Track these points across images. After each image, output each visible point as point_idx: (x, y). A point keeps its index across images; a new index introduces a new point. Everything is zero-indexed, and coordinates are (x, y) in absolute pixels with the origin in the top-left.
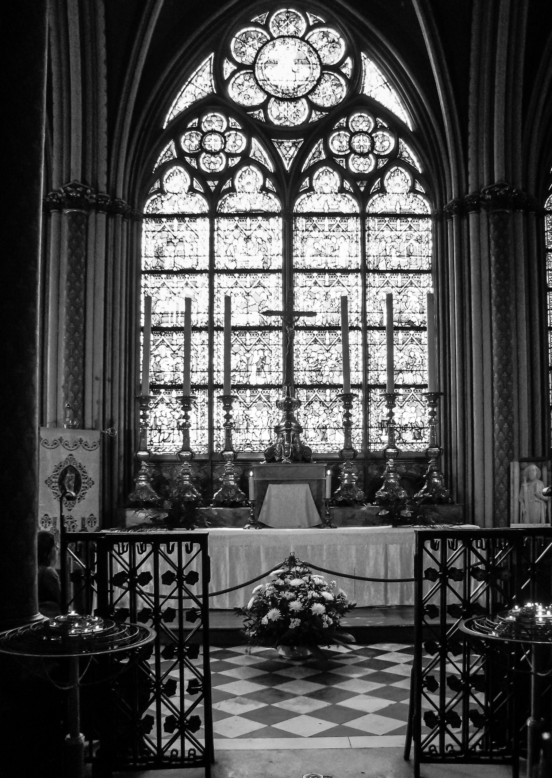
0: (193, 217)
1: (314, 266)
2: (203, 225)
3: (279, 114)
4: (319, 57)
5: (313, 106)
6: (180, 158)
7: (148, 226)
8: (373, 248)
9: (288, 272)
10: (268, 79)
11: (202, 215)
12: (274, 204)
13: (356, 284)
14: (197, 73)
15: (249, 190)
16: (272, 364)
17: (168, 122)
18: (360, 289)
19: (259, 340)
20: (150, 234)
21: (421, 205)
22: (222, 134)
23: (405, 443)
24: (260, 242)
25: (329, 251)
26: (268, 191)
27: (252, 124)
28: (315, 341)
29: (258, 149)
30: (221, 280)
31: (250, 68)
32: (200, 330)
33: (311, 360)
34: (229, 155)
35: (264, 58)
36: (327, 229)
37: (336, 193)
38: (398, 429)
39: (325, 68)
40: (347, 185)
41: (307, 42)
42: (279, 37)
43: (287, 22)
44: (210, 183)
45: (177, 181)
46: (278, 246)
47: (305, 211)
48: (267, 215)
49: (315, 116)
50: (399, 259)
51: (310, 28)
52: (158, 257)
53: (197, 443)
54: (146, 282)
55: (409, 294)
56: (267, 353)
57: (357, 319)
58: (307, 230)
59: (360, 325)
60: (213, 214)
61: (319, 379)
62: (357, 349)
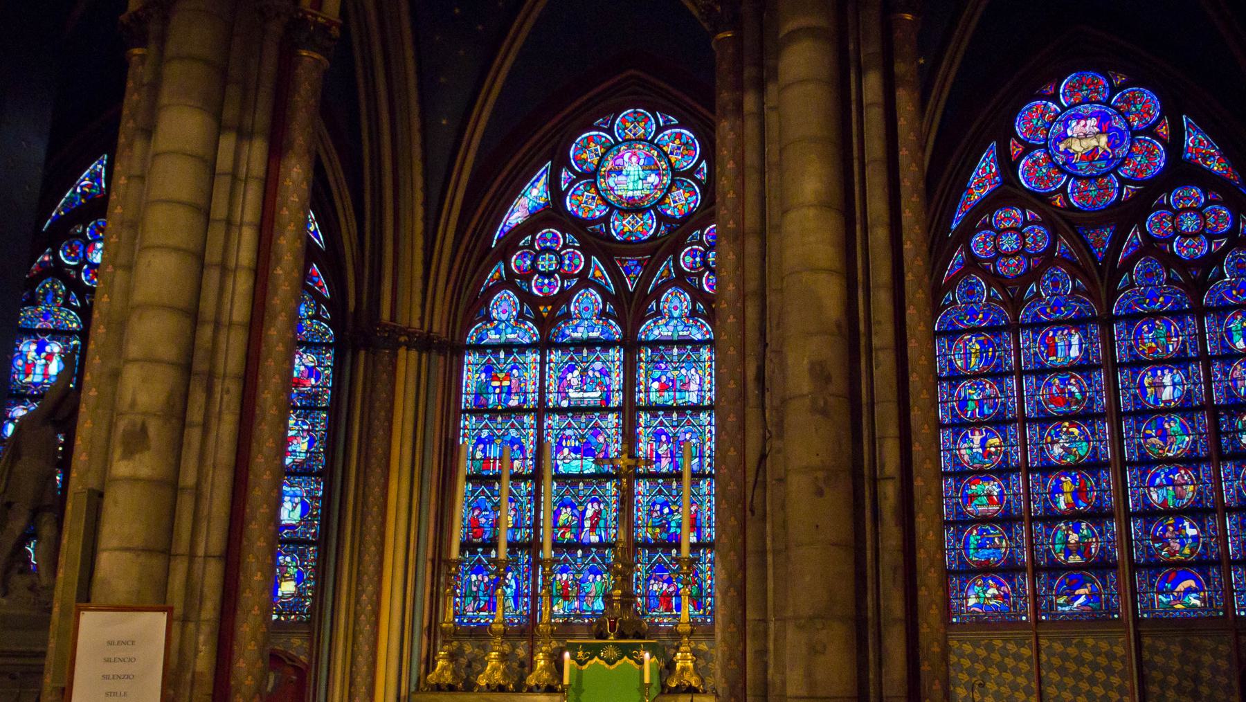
0: (522, 348)
1: (660, 401)
2: (532, 357)
3: (622, 226)
4: (669, 161)
5: (662, 218)
6: (508, 282)
9: (630, 411)
10: (612, 189)
11: (532, 346)
12: (616, 331)
15: (587, 317)
18: (713, 429)
19: (595, 491)
22: (557, 253)
24: (597, 374)
26: (609, 316)
27: (594, 238)
28: (660, 492)
29: (599, 270)
30: (554, 421)
31: (591, 176)
32: (525, 478)
33: (655, 515)
35: (608, 165)
36: (675, 359)
37: (688, 318)
39: (675, 172)
40: (700, 306)
41: (657, 145)
42: (625, 141)
43: (630, 122)
44: (542, 308)
45: (504, 305)
46: (616, 380)
47: (651, 338)
48: (607, 345)
57: (710, 465)
58: (652, 361)
60: (543, 346)
61: (665, 536)
62: (710, 501)
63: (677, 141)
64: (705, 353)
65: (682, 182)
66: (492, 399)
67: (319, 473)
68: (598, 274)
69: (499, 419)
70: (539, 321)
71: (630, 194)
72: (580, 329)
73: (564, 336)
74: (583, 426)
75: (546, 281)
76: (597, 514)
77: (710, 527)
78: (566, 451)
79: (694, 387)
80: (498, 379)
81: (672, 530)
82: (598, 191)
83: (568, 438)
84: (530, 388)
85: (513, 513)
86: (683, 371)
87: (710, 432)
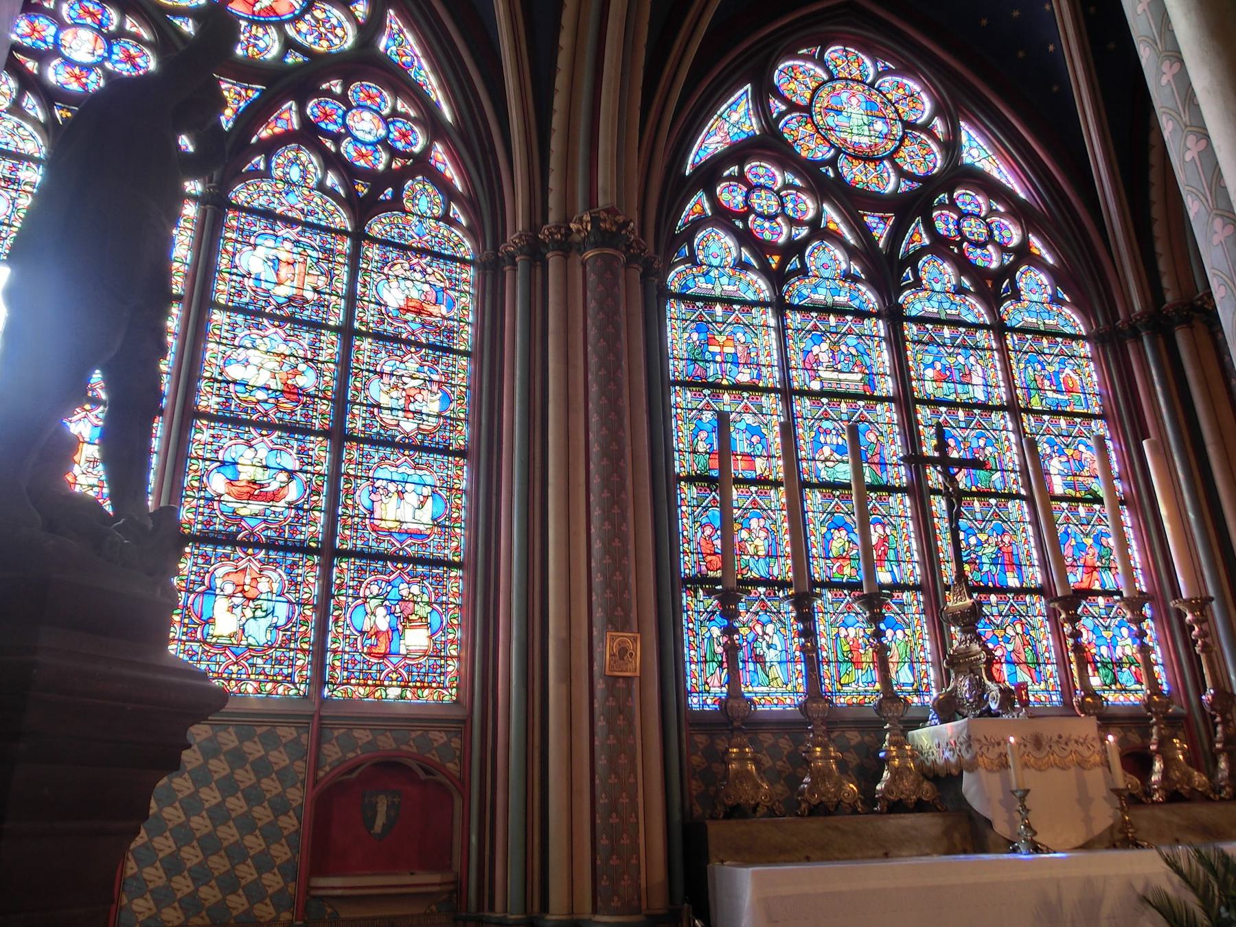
1: (939, 394)
4: (897, 111)
7: (674, 309)
8: (1023, 373)
12: (869, 298)
13: (1005, 428)
14: (730, 106)
16: (899, 548)
17: (693, 164)
20: (678, 324)
21: (1071, 320)
23: (1124, 690)
25: (957, 376)
27: (821, 182)
29: (832, 217)
34: (792, 222)
38: (1110, 666)
39: (908, 125)
40: (966, 283)
48: (861, 314)
49: (904, 186)
50: (1055, 396)
51: (879, 75)
52: (695, 361)
53: (789, 687)
54: (679, 399)
55: (1082, 448)
56: (888, 531)
57: (1016, 482)
59: (1023, 492)
62: (1024, 531)
63: (901, 90)
64: (984, 338)
65: (915, 138)
66: (712, 369)
67: (461, 453)
68: (832, 226)
69: (726, 397)
70: (765, 271)
71: (856, 139)
72: (821, 291)
73: (800, 296)
74: (845, 417)
75: (767, 225)
76: (885, 539)
77: (1032, 565)
78: (827, 451)
79: (976, 379)
80: (718, 344)
81: (985, 568)
82: (816, 126)
83: (827, 432)
84: (763, 360)
85: (763, 534)
86: (961, 359)
87: (1008, 439)
